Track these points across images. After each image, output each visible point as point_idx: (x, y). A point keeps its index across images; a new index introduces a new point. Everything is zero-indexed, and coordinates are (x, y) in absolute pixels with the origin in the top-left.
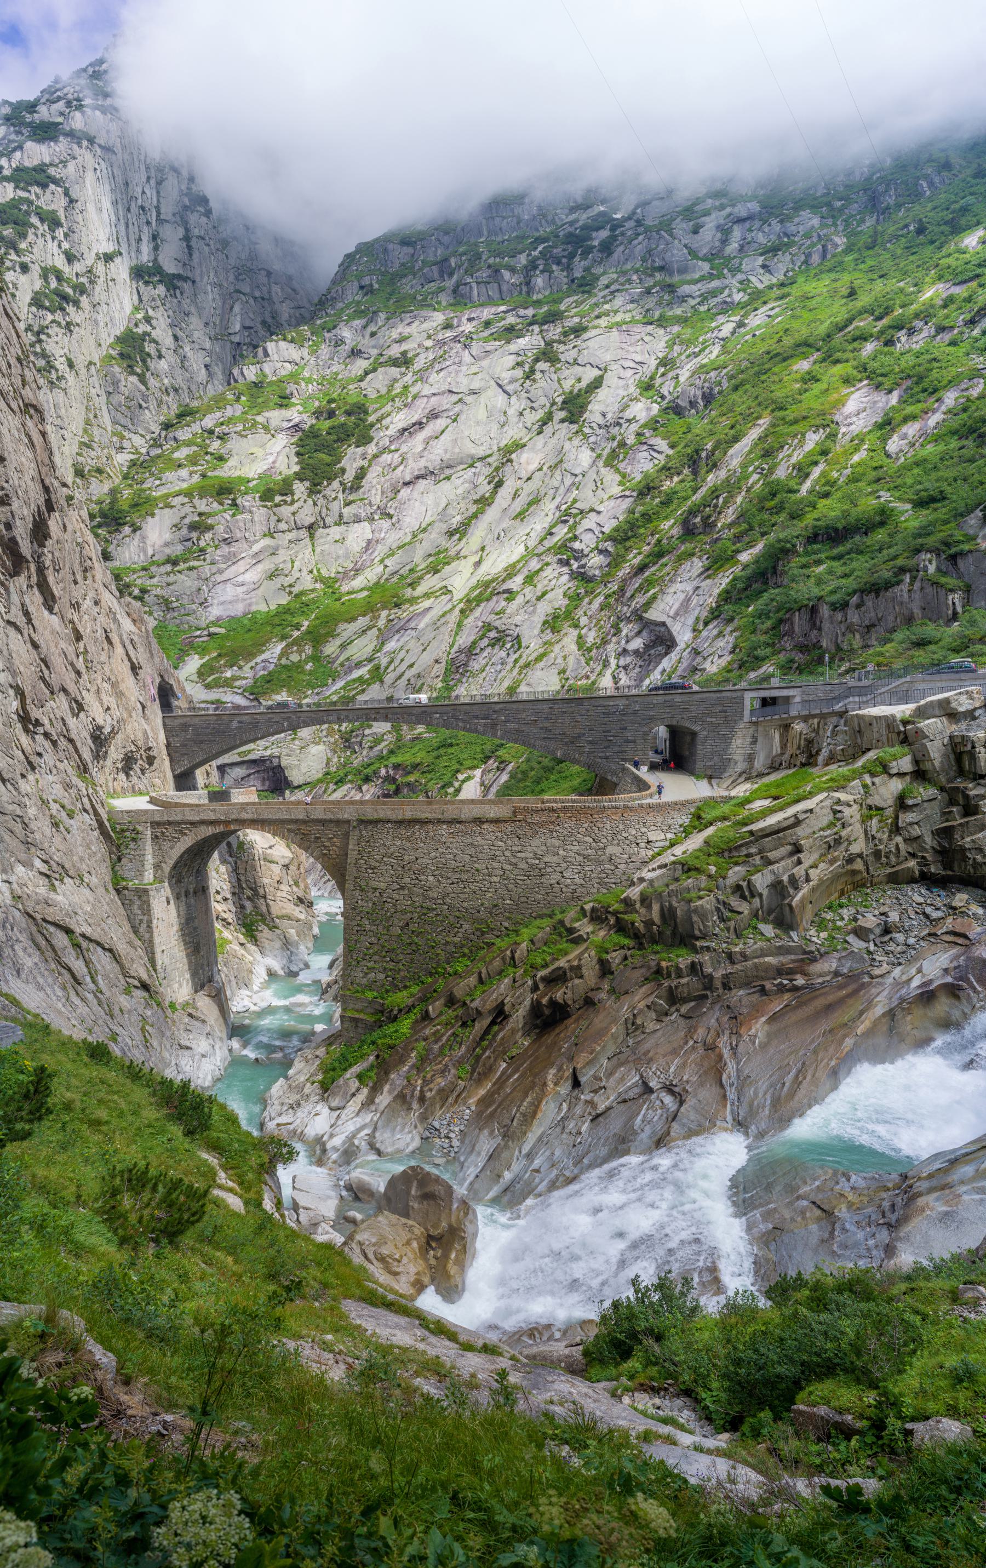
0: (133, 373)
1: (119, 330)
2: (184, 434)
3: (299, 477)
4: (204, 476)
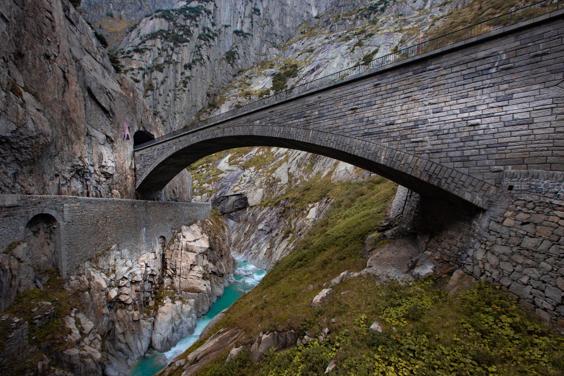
0: (230, 63)
1: (227, 50)
2: (239, 78)
3: (272, 89)
4: (243, 90)
